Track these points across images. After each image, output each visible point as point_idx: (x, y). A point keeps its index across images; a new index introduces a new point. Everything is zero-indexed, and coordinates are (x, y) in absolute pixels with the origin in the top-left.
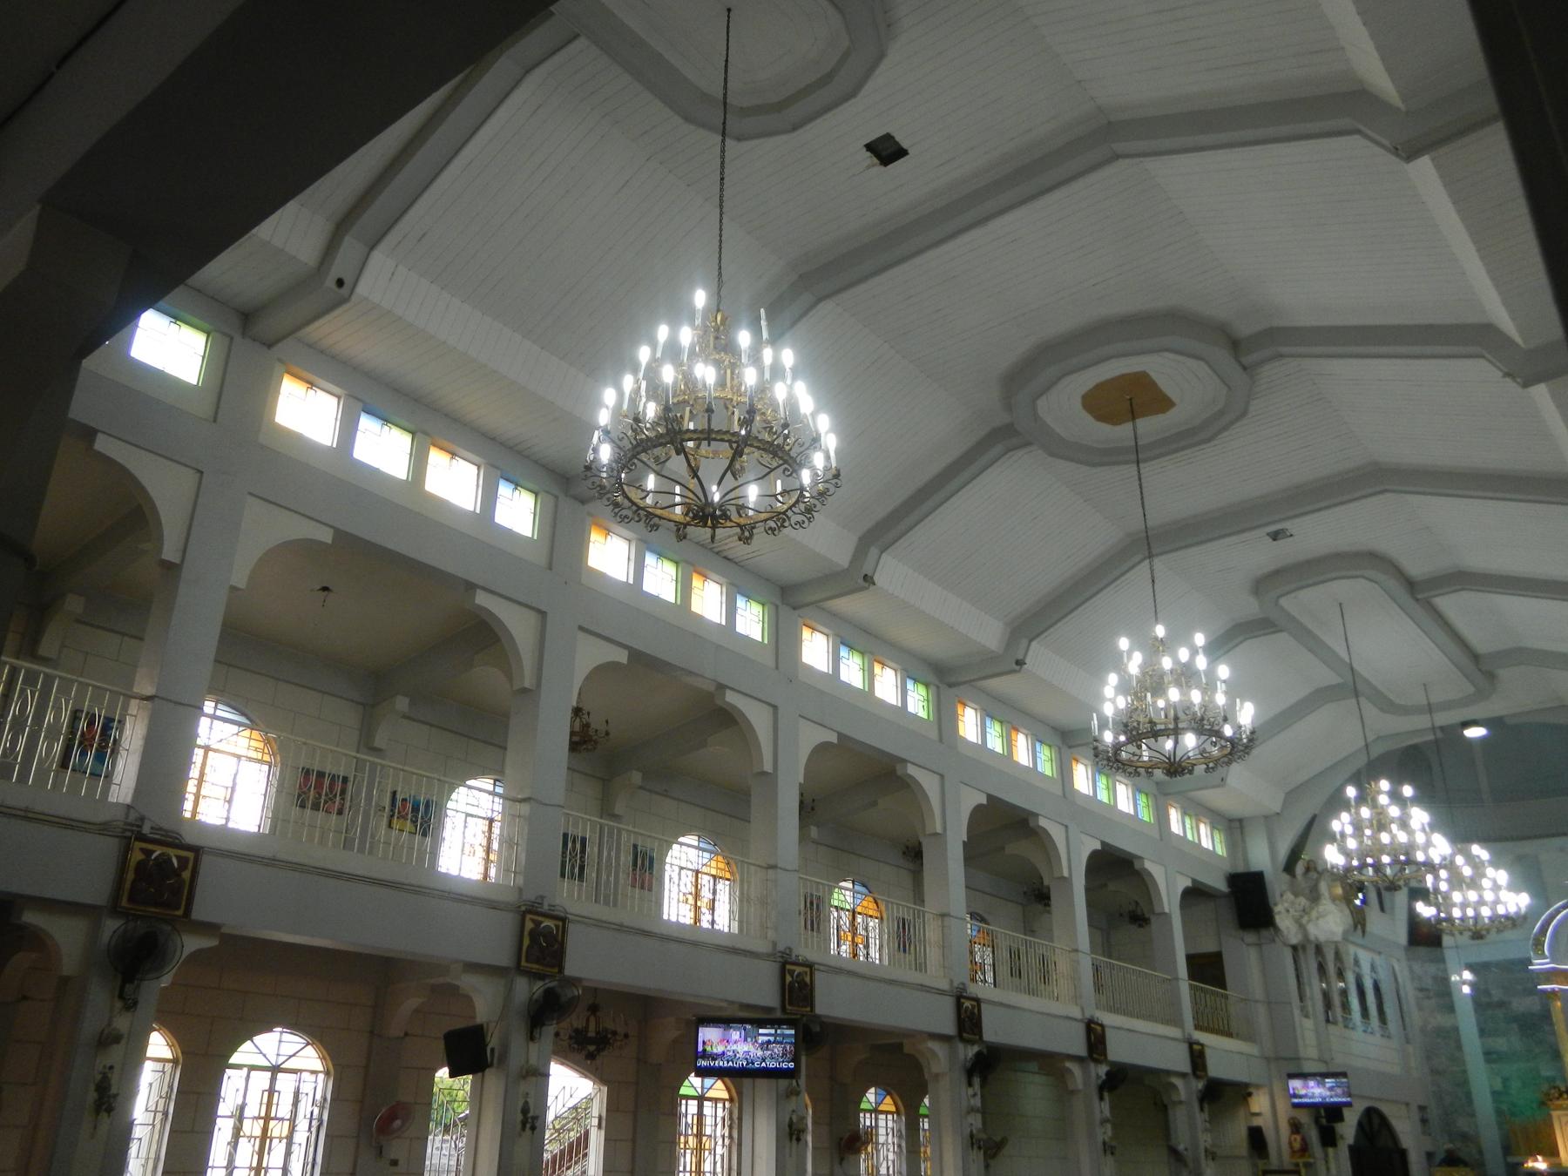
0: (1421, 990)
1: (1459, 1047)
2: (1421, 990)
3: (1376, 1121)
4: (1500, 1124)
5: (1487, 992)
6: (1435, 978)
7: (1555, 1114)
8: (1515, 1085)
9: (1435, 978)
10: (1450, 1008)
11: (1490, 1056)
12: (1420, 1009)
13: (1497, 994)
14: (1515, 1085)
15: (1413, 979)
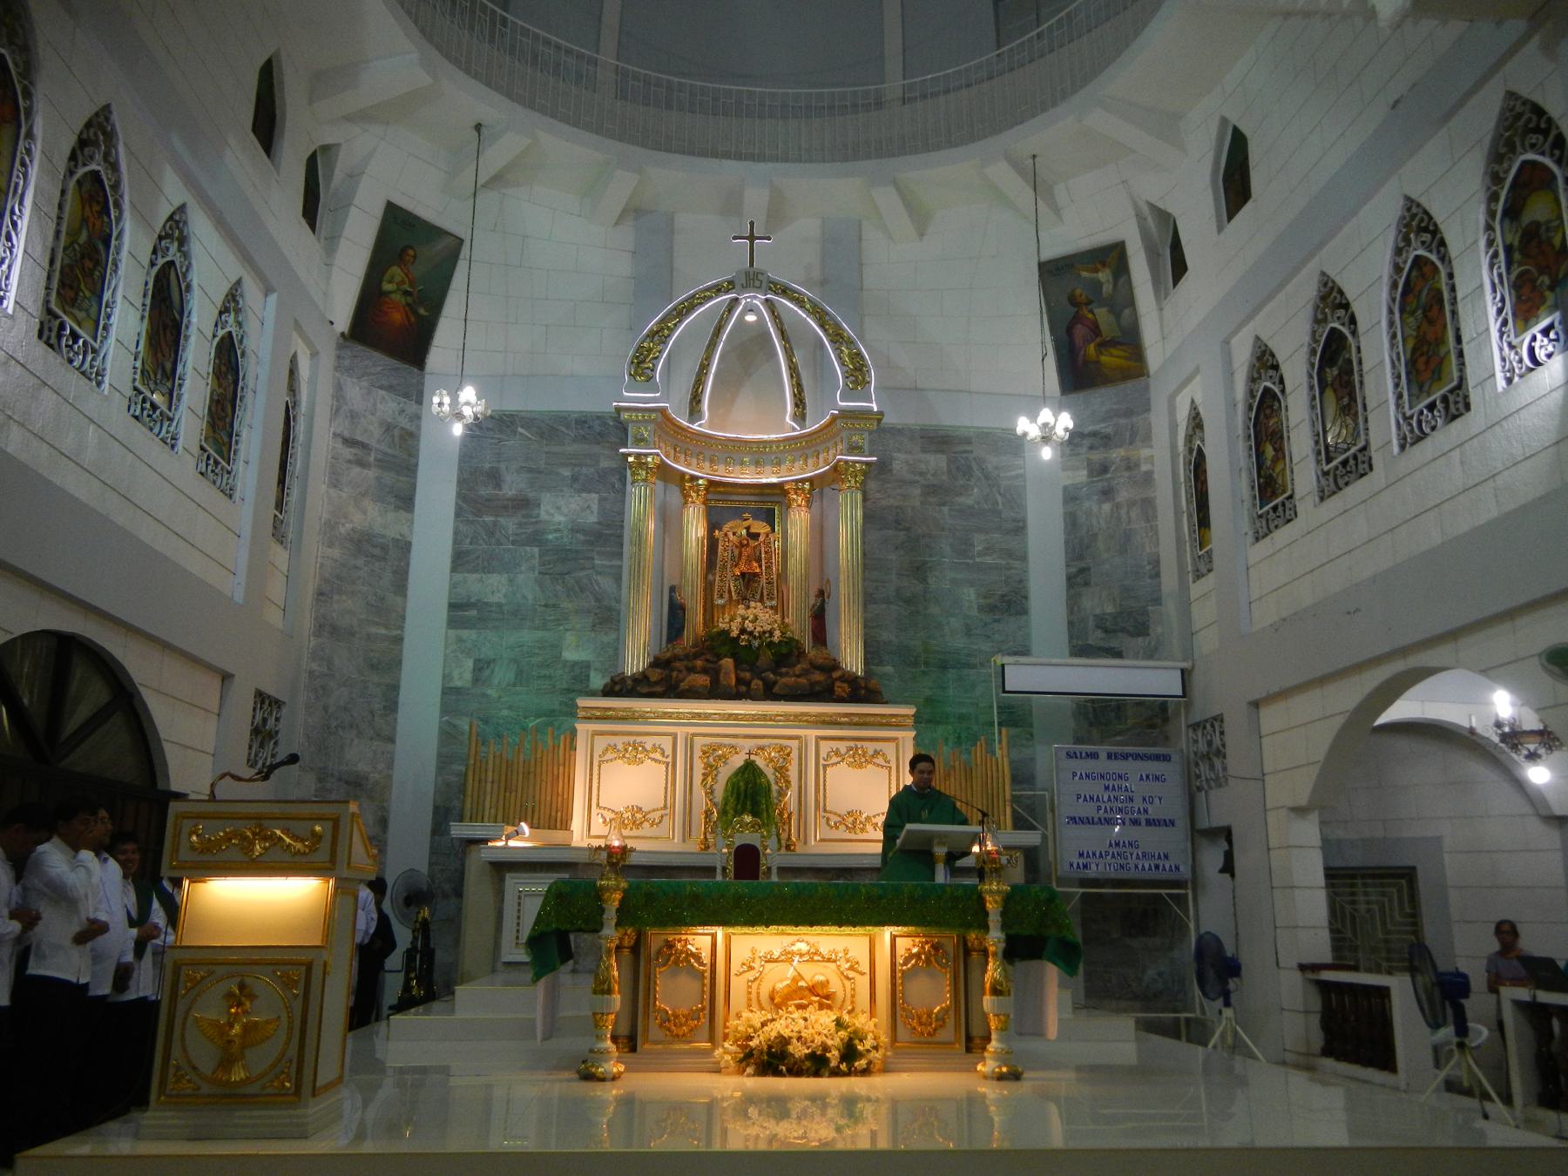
0: (350, 442)
1: (401, 586)
2: (350, 442)
3: (89, 695)
4: (444, 761)
5: (495, 477)
6: (388, 428)
7: (583, 729)
8: (503, 674)
9: (388, 428)
10: (406, 501)
11: (461, 612)
12: (335, 483)
13: (513, 484)
14: (503, 674)
15: (336, 412)
